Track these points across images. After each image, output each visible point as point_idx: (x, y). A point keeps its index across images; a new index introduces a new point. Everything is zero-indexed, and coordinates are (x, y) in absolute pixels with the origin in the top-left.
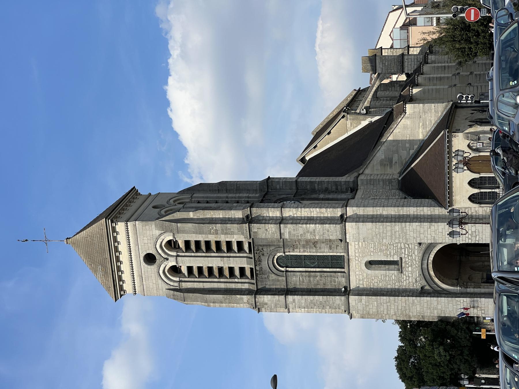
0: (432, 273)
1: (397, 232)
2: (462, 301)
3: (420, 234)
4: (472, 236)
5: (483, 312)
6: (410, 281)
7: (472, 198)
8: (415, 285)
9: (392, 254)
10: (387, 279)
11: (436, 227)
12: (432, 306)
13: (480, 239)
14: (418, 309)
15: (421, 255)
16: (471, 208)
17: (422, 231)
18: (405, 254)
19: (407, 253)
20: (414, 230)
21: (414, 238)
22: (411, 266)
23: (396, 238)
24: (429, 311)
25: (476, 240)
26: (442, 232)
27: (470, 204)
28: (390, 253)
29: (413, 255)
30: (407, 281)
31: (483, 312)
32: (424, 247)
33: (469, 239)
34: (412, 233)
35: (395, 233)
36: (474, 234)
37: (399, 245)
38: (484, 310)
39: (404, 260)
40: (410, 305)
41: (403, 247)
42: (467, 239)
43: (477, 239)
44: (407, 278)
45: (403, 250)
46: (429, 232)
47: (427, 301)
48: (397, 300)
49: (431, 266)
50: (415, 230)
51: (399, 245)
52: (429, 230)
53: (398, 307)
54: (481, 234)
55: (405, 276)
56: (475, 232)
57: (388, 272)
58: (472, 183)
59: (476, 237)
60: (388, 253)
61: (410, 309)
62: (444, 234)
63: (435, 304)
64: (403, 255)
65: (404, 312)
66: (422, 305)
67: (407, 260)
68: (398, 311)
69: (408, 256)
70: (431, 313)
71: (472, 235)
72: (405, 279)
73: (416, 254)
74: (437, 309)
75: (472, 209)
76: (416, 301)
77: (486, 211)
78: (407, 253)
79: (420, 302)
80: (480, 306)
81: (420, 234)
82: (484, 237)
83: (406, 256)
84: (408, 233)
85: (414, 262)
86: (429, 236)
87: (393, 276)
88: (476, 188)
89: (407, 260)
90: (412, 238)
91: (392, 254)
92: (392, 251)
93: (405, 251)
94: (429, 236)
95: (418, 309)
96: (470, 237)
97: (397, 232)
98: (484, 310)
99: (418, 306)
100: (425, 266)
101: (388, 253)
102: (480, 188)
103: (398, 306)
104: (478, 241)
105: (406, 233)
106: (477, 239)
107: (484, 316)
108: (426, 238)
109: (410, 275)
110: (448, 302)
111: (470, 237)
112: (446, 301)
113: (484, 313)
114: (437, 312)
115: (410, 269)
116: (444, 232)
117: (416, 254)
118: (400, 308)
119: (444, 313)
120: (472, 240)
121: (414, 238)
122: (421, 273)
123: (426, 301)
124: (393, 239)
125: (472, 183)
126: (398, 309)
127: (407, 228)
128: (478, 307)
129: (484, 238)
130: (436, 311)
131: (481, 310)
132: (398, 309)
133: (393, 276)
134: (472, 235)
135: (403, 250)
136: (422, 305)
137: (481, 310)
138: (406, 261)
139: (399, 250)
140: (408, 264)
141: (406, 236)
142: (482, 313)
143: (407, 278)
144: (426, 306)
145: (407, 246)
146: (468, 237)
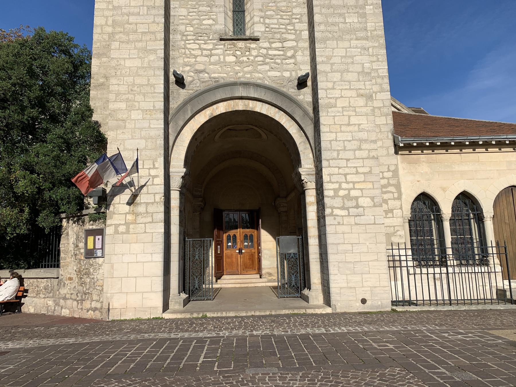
0: (221, 108)
1: (342, 20)
2: (153, 172)
3: (342, 72)
4: (343, 197)
5: (122, 229)
6: (199, 59)
7: (425, 202)
8: (188, 68)
9: (267, 21)
10: (201, 8)
11: (364, 110)
12: (139, 98)
13: (339, 219)
14: (128, 63)
15: (267, 83)
16: (399, 198)
17: (349, 76)
18: (267, 49)
19: (270, 52)
20: (352, 57)
21: (329, 58)
22: (238, 62)
23: (326, 16)
24: (123, 89)
25: (332, 208)
26: (349, 125)
27: (409, 195)
28: (270, 17)
29: (267, 67)
30: (199, 52)
31: (122, 229)
32: (292, 91)
33: (336, 191)
34: (342, 53)
35: (340, 15)
36: (349, 204)
37: (293, 37)
38: (128, 232)
39: (253, 45)
40: (139, 45)
41: (286, 44)
42: (336, 186)
43: (337, 212)
44: (205, 52)
45: (278, 45)
46: (349, 93)
47: (153, 86)
48: (153, 12)
49: (240, 106)
50: (350, 60)
51: (293, 37)
52: (354, 93)
53: (133, 14)
54: (352, 220)
55: (211, 47)
56: (357, 207)
57: (222, 9)
58: (466, 200)
59: (343, 208)
60: (269, 13)
61: (128, 42)
62: (344, 128)
63: (144, 105)
64: (266, 45)
65: (118, 29)
66: (141, 72)
67: (254, 53)
68: (123, 14)
69: (265, 56)
70: (118, 94)
71: (348, 197)
72: (205, 46)
73: (270, 74)
74: (130, 108)
75: (397, 203)
76: (152, 57)
77: (394, 234)
78: (270, 52)
79: (150, 67)
80: (140, 220)
81: (342, 72)
82: (346, 229)
83: (264, 51)
84: (341, 44)
85: (250, 68)
86: (336, 93)
87: (211, 22)
88: (454, 208)
89: (254, 53)
90: (328, 52)
91: (267, 21)
92: (275, 21)
93: (277, 49)
94: (336, 93)
95: (128, 63)
96: (342, 193)
97: (342, 20)
98: (128, 232)
99: (137, 63)
100: (241, 92)
101: (269, 13)
102: (452, 221)
103: (138, 14)
104: (331, 214)
105: (340, 38)
106: (337, 212)
107: (109, 231)
108: (330, 85)
109: (214, 59)
110: (151, 138)
111: (342, 193)
112: (153, 133)
113: (116, 232)
114: (120, 110)
115: (233, 59)
116: (351, 128)
117: (270, 74)
118: (132, 19)
119: (118, 128)
120: (333, 197)
121: (329, 58)
122: (222, 81)
123: (153, 81)
124: (323, 10)
125: (466, 200)
126: (129, 14)
127: (354, 43)
128: (137, 215)
129: (340, 229)
130: (123, 105)
131: (127, 224)
132: (129, 14)
133: (211, 22)
134: (348, 197)
135: (278, 45)
136: (141, 72)
137: (127, 224)
138: (249, 50)
139: (278, 36)
140: (243, 55)
141: (333, 38)
142: (117, 226)
143: (205, 52)
144: (138, 81)
145: (289, 54)
146: (340, 188)
